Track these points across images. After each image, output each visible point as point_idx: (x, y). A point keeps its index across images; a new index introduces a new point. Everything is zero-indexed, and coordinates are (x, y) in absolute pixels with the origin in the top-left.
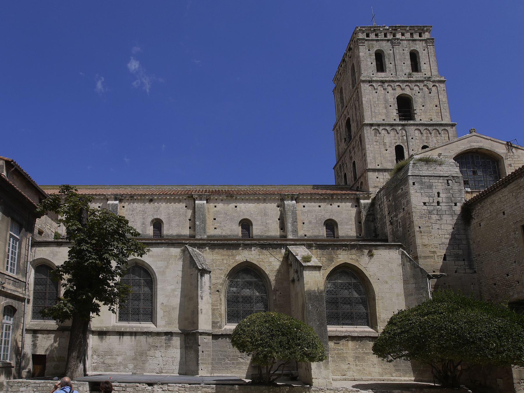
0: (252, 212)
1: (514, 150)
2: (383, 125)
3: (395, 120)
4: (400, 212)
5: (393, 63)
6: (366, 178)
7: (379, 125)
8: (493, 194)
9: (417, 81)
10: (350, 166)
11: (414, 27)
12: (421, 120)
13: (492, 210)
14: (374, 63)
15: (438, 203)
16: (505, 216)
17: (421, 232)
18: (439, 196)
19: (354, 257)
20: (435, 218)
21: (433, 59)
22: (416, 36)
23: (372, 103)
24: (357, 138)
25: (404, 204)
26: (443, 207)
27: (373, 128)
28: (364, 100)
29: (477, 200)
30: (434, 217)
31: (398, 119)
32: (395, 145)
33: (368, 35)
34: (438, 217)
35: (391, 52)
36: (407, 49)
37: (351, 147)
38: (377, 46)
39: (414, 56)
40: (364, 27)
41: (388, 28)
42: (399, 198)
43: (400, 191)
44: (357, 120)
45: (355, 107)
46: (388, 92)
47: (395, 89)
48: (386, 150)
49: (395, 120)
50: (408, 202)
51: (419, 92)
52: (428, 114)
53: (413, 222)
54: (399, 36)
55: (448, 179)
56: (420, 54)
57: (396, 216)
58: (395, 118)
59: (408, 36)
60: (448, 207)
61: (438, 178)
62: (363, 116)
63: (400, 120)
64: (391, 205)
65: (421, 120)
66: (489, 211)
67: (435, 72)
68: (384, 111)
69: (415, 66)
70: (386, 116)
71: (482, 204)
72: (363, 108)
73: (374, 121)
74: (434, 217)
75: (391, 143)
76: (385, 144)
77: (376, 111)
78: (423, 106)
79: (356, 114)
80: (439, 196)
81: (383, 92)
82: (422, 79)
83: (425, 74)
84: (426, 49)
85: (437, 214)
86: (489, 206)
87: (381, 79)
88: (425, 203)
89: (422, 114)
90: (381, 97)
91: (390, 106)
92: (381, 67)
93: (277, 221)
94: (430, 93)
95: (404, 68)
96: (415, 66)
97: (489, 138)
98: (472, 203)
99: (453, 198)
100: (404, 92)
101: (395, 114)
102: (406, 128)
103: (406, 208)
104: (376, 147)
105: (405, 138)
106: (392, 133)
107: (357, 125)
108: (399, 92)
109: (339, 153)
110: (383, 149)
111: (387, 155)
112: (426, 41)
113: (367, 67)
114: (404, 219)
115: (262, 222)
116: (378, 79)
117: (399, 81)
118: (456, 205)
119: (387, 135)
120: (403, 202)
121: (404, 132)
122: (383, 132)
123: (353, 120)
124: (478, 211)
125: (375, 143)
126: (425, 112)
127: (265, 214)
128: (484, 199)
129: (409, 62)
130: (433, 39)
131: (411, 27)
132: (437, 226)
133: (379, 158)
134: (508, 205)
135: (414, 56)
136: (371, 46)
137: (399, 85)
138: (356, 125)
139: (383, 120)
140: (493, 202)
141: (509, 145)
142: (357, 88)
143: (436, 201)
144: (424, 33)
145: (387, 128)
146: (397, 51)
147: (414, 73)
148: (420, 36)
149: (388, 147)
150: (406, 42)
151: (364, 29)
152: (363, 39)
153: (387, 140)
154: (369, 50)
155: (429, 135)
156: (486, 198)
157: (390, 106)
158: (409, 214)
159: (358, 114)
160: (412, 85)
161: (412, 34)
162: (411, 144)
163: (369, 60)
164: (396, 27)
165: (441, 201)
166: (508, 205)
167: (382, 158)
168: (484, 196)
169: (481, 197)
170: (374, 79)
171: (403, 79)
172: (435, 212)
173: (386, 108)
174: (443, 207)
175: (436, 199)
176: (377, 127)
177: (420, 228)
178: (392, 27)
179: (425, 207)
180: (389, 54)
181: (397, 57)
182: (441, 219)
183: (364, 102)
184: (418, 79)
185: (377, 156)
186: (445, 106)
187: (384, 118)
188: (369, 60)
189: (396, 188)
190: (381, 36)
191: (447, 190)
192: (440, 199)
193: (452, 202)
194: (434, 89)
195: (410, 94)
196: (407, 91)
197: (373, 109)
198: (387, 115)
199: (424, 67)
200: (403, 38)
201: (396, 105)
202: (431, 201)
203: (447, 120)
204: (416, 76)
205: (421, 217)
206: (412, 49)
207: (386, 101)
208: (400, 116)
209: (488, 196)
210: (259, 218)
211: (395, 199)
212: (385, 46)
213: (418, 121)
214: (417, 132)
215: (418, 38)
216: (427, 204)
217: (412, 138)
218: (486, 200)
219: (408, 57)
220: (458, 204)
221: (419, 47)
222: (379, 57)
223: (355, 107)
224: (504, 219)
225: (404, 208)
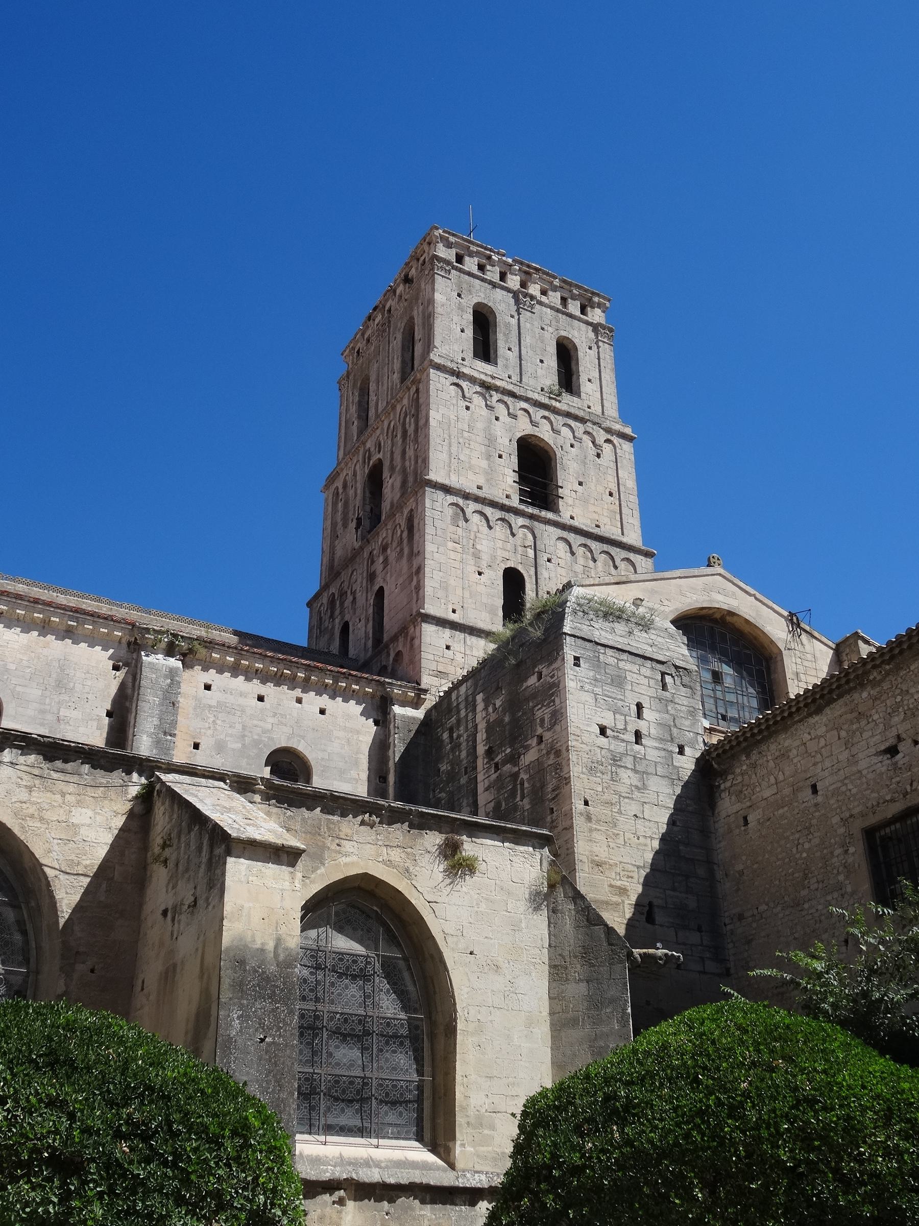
0: (12, 667)
1: (804, 637)
2: (477, 499)
4: (527, 748)
5: (516, 349)
6: (416, 642)
7: (467, 496)
8: (786, 729)
9: (568, 415)
10: (365, 600)
11: (570, 284)
12: (572, 518)
13: (781, 777)
14: (469, 332)
15: (638, 735)
16: (819, 799)
17: (589, 818)
18: (639, 715)
19: (396, 855)
20: (628, 782)
21: (609, 377)
22: (574, 307)
23: (454, 432)
24: (401, 519)
25: (542, 720)
26: (651, 750)
27: (451, 499)
28: (435, 416)
29: (739, 743)
30: (627, 777)
32: (504, 566)
34: (635, 780)
35: (514, 321)
37: (375, 546)
38: (480, 294)
39: (566, 354)
40: (453, 235)
41: (510, 260)
42: (527, 700)
43: (532, 680)
44: (404, 471)
45: (405, 432)
46: (497, 419)
47: (515, 417)
48: (480, 574)
49: (508, 496)
50: (558, 717)
51: (572, 446)
52: (592, 508)
53: (568, 780)
54: (534, 289)
55: (666, 670)
56: (580, 354)
57: (514, 759)
58: (510, 491)
59: (555, 298)
60: (663, 753)
61: (639, 661)
62: (426, 461)
63: (521, 501)
64: (499, 722)
66: (772, 780)
67: (612, 410)
68: (484, 464)
69: (568, 378)
70: (487, 480)
71: (754, 757)
72: (427, 436)
73: (453, 481)
74: (627, 777)
75: (494, 557)
76: (477, 556)
77: (462, 457)
79: (404, 453)
80: (639, 715)
81: (485, 412)
84: (595, 348)
85: (635, 771)
86: (771, 764)
87: (483, 377)
88: (603, 731)
90: (480, 425)
91: (500, 456)
92: (484, 349)
93: (99, 719)
94: (598, 456)
95: (539, 371)
96: (568, 378)
97: (752, 591)
98: (725, 751)
99: (675, 730)
102: (539, 527)
103: (547, 736)
104: (452, 555)
105: (531, 553)
106: (500, 531)
107: (404, 483)
108: (523, 427)
109: (332, 560)
110: (471, 569)
111: (481, 589)
112: (596, 327)
113: (452, 338)
114: (538, 770)
115: (43, 712)
116: (476, 375)
117: (527, 400)
118: (681, 751)
119: (485, 529)
120: (539, 714)
121: (530, 536)
122: (476, 519)
123: (392, 468)
124: (740, 779)
125: (451, 545)
126: (585, 501)
127: (61, 685)
128: (760, 742)
129: (552, 362)
130: (611, 330)
131: (564, 281)
132: (632, 808)
133: (459, 592)
134: (828, 763)
135: (566, 354)
136: (464, 286)
137: (526, 410)
138: (398, 484)
139: (479, 488)
140: (784, 755)
141: (794, 622)
142: (417, 382)
143: (632, 728)
144: (593, 307)
145: (488, 511)
146: (528, 325)
148: (583, 310)
149: (484, 564)
151: (452, 239)
152: (448, 263)
153: (484, 546)
154: (459, 295)
155: (591, 563)
156: (764, 740)
157: (500, 456)
158: (558, 753)
159: (410, 453)
160: (558, 421)
161: (564, 300)
162: (544, 574)
163: (456, 319)
164: (529, 266)
165: (644, 731)
166: (828, 763)
167: (467, 594)
168: (760, 732)
169: (753, 735)
170: (466, 371)
171: (536, 396)
172: (628, 762)
173: (489, 457)
174: (651, 750)
175: (634, 724)
176: (461, 501)
177: (586, 803)
178: (521, 263)
179: (602, 741)
180: (508, 325)
181: (527, 340)
182: (645, 787)
183: (432, 423)
184: (572, 411)
185: (452, 582)
186: (631, 500)
187: (481, 482)
188: (456, 319)
189: (521, 671)
190: (493, 274)
191: (664, 703)
192: (642, 726)
193: (672, 740)
194: (607, 448)
195: (551, 442)
196: (544, 432)
197: (454, 449)
198: (490, 474)
199: (588, 388)
200: (544, 299)
201: (515, 459)
202: (620, 726)
203: (633, 537)
204: (567, 402)
205: (592, 770)
206: (563, 333)
207: (491, 441)
208: (522, 492)
209: (770, 736)
210: (34, 692)
211: (515, 704)
212: (501, 304)
213: (565, 518)
214: (562, 545)
215: (577, 313)
216: (609, 732)
217: (549, 560)
218: (764, 747)
219: (552, 349)
220: (686, 749)
221: (581, 336)
222: (483, 321)
223: (405, 432)
224: (816, 805)
225: (540, 739)
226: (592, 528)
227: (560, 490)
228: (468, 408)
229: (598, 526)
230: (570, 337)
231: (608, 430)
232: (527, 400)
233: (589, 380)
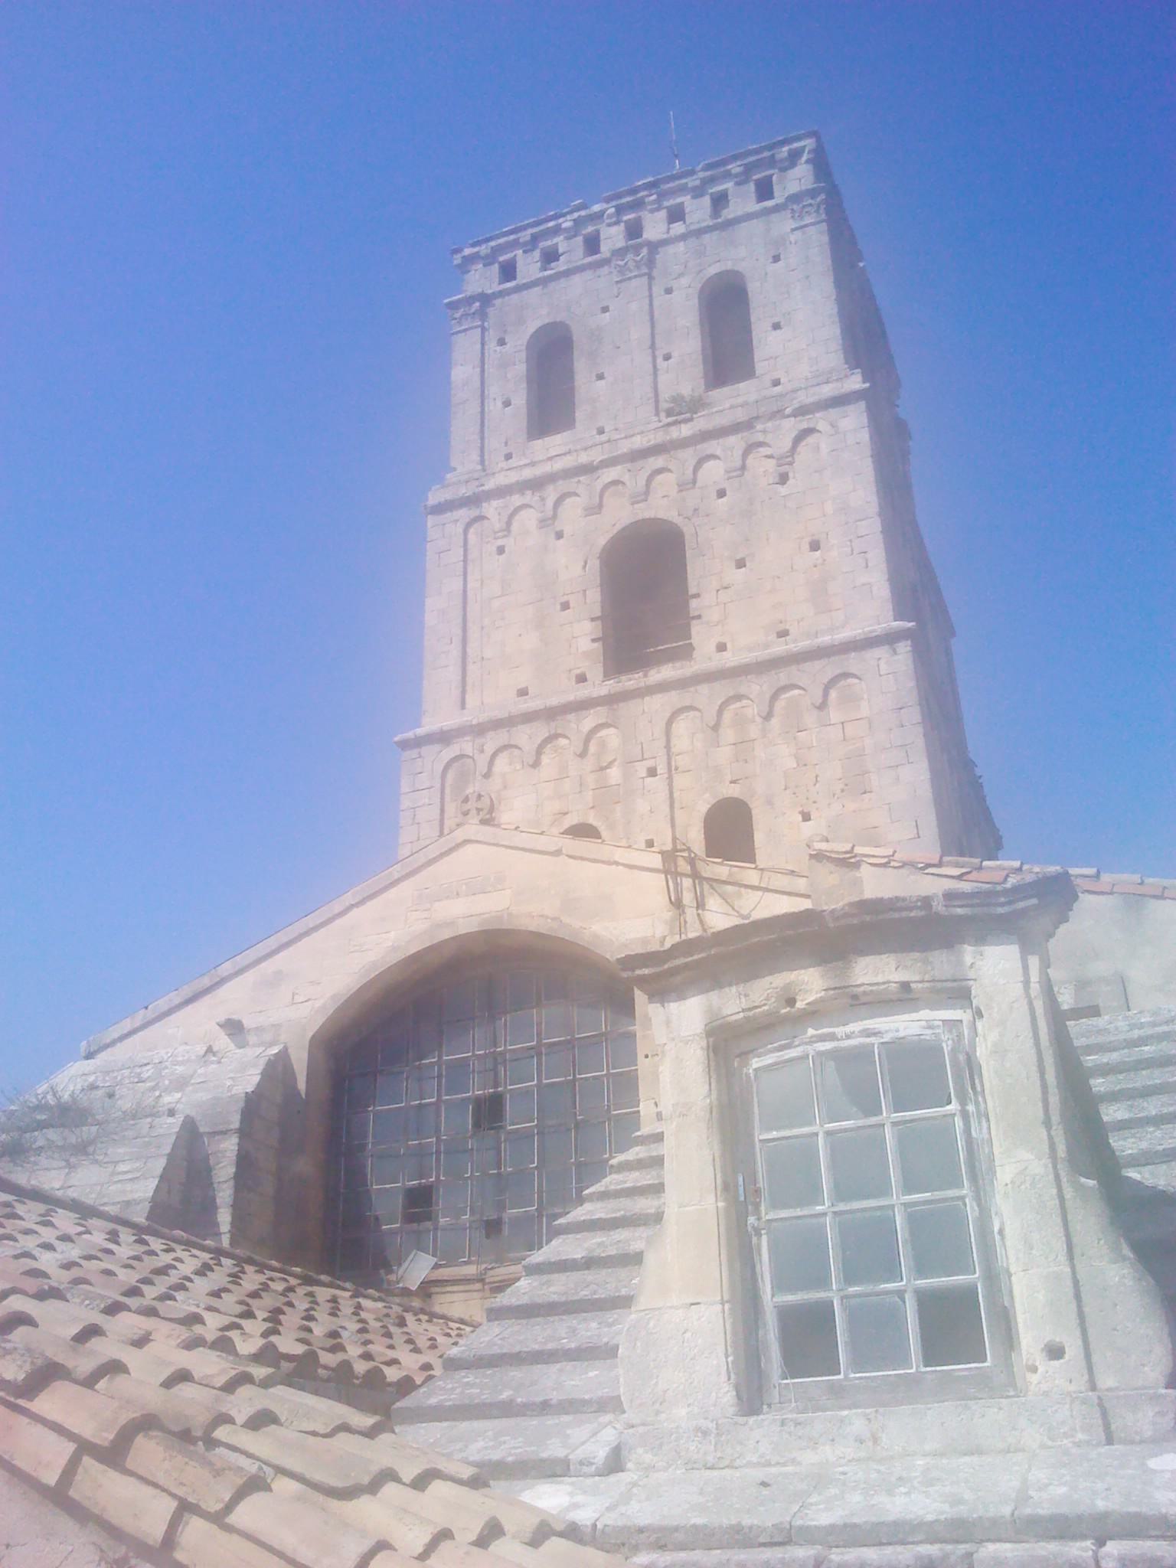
3: (582, 679)
31: (595, 673)
33: (508, 271)
36: (684, 281)
38: (534, 311)
41: (596, 208)
49: (582, 679)
51: (721, 494)
58: (583, 666)
65: (722, 647)
78: (741, 564)
82: (741, 415)
83: (776, 383)
89: (728, 619)
91: (565, 606)
94: (783, 479)
100: (645, 512)
101: (585, 644)
108: (619, 515)
137: (616, 483)
139: (523, 692)
147: (717, 394)
148: (765, 191)
150: (681, 247)
164: (633, 191)
188: (493, 390)
201: (595, 596)
204: (732, 400)
221: (743, 253)
226: (767, 646)
227: (694, 604)
228: (501, 550)
229: (783, 634)
230: (729, 266)
231: (802, 411)
232: (612, 462)
233: (776, 326)
